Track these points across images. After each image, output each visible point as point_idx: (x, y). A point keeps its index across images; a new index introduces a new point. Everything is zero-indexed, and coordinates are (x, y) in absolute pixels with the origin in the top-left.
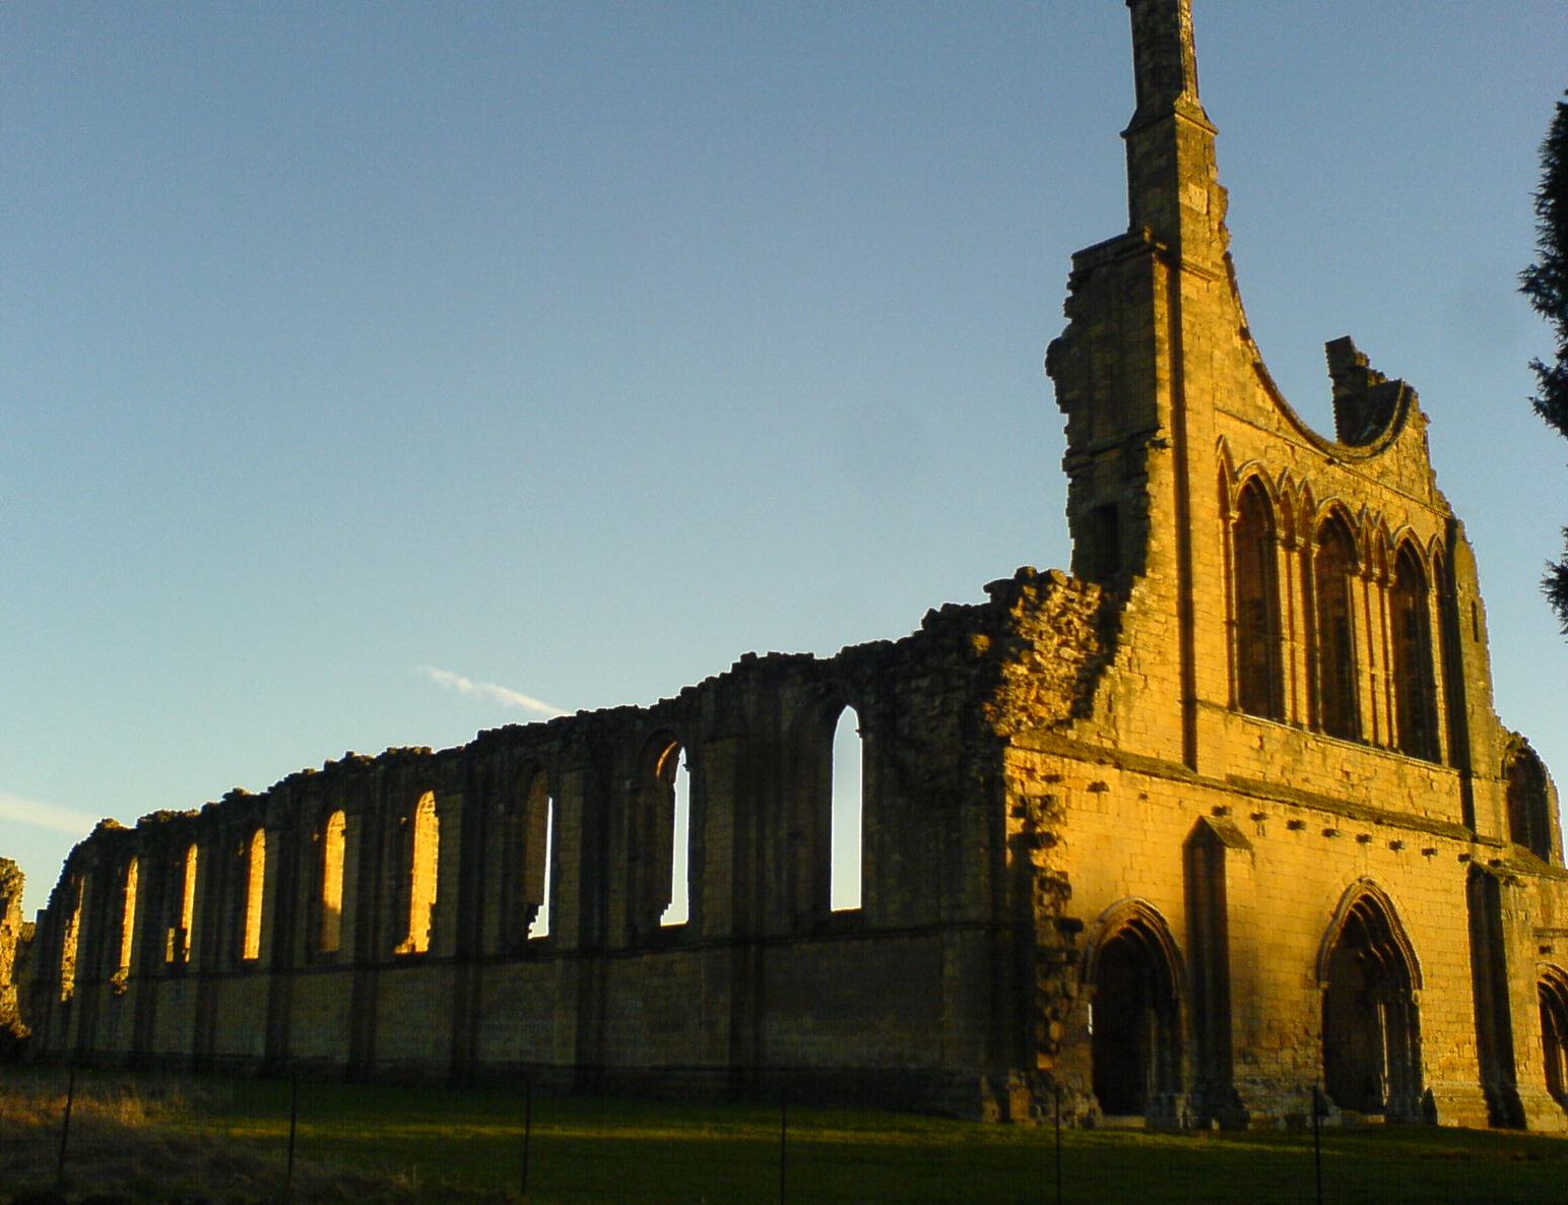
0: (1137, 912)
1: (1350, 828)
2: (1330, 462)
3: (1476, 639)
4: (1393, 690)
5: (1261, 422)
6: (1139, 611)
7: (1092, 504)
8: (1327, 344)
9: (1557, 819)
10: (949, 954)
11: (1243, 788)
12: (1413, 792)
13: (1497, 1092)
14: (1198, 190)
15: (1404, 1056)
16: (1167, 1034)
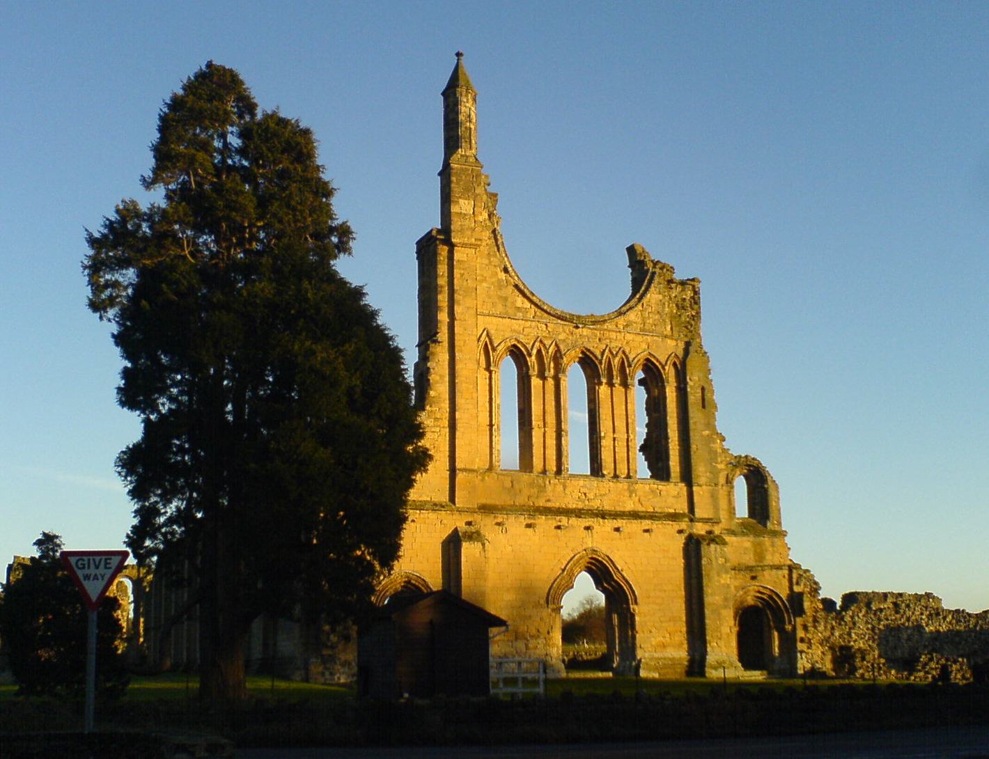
0: (408, 577)
2: (577, 327)
8: (627, 249)
9: (778, 503)
12: (642, 498)
13: (697, 657)
14: (466, 202)
15: (626, 642)
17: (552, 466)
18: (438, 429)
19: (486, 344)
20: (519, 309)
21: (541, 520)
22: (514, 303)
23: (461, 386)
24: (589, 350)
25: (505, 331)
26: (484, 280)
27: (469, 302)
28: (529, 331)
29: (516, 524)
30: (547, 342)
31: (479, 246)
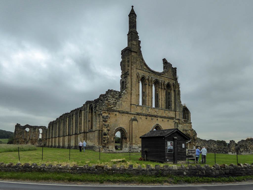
1: (155, 119)
3: (178, 95)
4: (165, 102)
5: (145, 70)
6: (124, 94)
7: (122, 81)
10: (96, 133)
11: (138, 114)
16: (126, 142)
17: (150, 104)
18: (127, 94)
19: (138, 76)
20: (144, 69)
21: (148, 117)
22: (144, 67)
23: (133, 85)
24: (158, 80)
25: (141, 73)
26: (138, 61)
27: (135, 65)
28: (147, 75)
29: (144, 118)
30: (150, 77)
31: (137, 52)
